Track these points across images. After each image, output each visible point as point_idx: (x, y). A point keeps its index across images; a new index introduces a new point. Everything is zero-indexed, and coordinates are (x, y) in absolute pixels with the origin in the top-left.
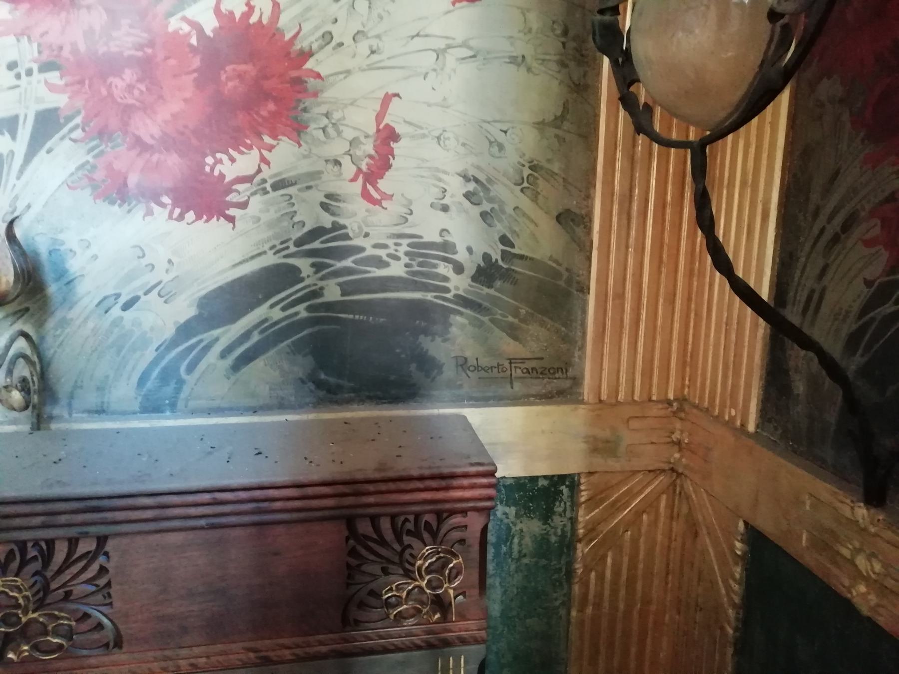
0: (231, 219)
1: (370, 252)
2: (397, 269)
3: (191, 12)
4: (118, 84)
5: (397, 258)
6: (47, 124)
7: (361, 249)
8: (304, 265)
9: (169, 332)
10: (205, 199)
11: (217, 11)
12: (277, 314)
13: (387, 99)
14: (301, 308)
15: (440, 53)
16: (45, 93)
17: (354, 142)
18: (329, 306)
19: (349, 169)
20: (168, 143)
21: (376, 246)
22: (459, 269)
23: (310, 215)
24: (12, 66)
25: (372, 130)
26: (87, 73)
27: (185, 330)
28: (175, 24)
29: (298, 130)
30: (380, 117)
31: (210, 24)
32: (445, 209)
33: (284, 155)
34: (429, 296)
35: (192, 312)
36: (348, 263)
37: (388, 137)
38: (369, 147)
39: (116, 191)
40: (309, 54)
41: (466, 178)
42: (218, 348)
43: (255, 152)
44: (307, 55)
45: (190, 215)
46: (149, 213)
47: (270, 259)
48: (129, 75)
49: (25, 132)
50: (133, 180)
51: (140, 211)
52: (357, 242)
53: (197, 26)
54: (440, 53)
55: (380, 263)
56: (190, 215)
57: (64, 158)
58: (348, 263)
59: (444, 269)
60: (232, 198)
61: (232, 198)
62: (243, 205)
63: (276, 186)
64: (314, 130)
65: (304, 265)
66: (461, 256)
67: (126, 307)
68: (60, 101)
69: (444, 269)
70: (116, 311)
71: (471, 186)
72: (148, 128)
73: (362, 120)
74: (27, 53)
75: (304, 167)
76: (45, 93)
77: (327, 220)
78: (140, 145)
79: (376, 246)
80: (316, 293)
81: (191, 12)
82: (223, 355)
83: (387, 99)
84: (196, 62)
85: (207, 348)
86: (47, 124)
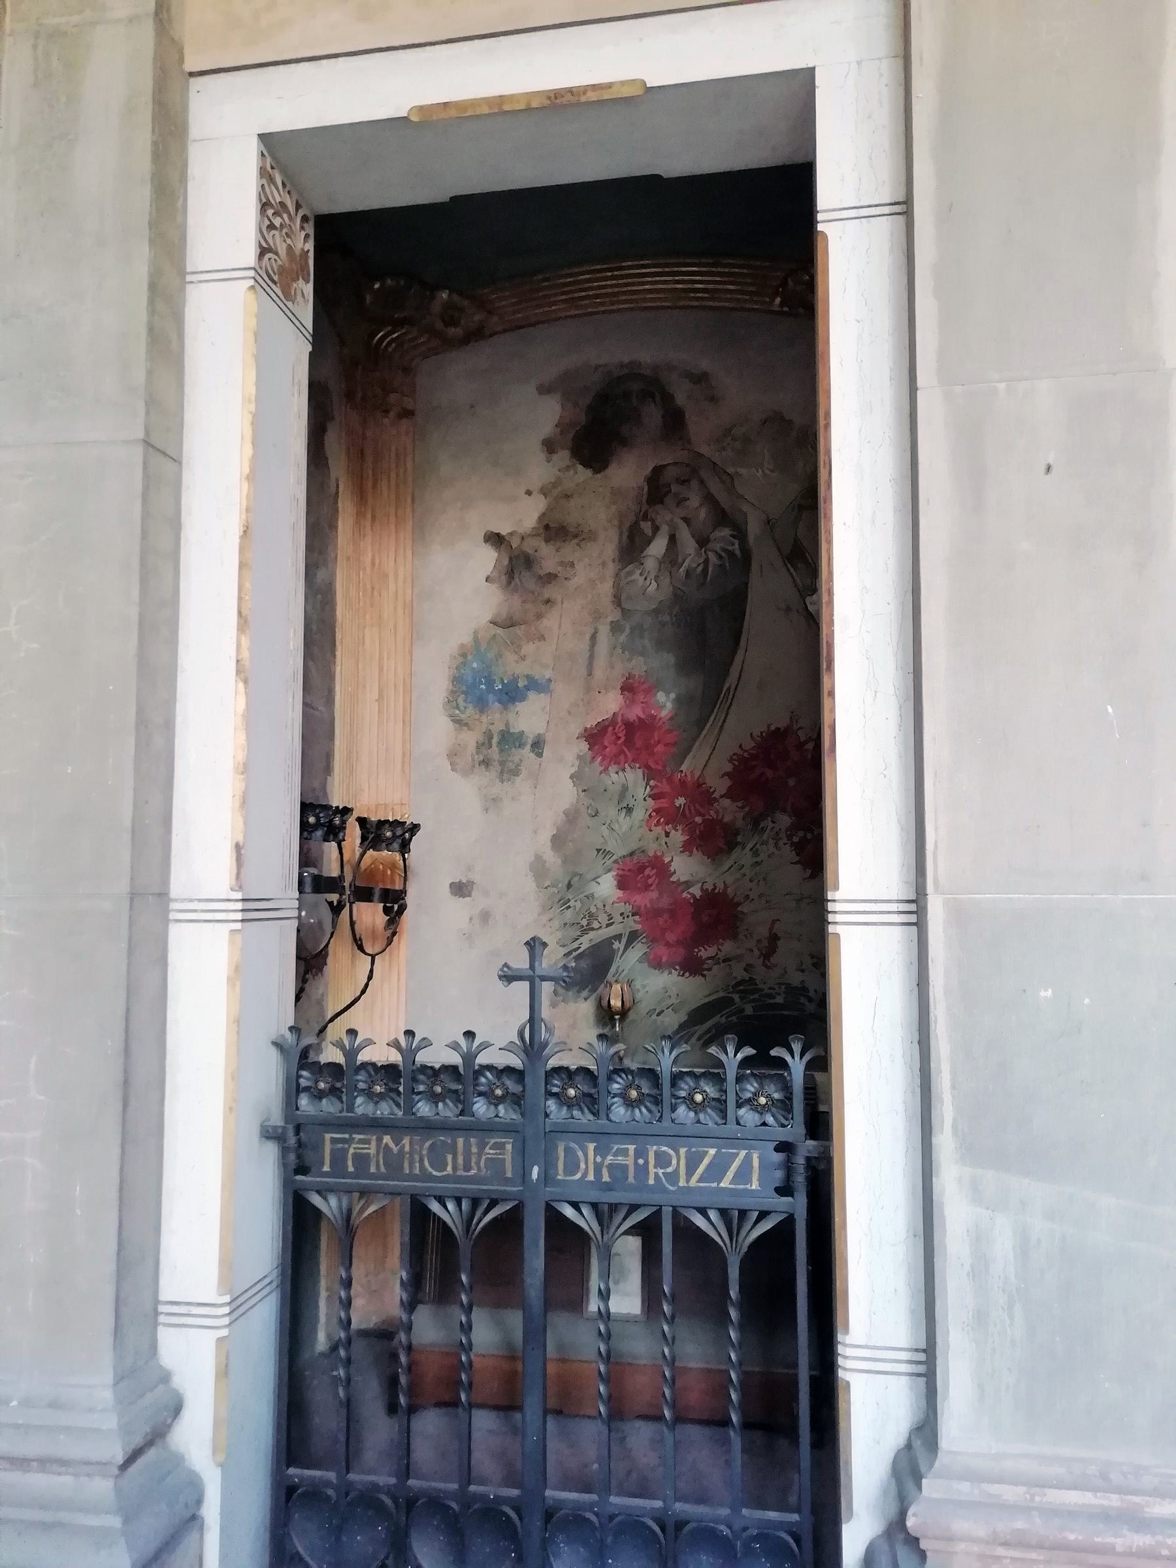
0: (704, 976)
1: (766, 991)
2: (779, 1000)
3: (690, 890)
4: (661, 921)
5: (779, 994)
6: (633, 937)
7: (762, 990)
8: (736, 997)
9: (676, 1027)
10: (692, 967)
11: (702, 889)
12: (723, 1020)
13: (774, 922)
14: (734, 1018)
15: (799, 901)
16: (633, 924)
17: (759, 941)
18: (748, 1017)
19: (756, 952)
20: (679, 942)
21: (770, 988)
22: (810, 1000)
23: (739, 973)
24: (622, 914)
25: (767, 935)
26: (648, 915)
27: (682, 1027)
28: (684, 895)
29: (734, 937)
30: (771, 929)
31: (698, 893)
32: (803, 971)
33: (728, 947)
34: (796, 1013)
35: (685, 1018)
36: (756, 996)
37: (774, 938)
38: (765, 943)
39: (657, 964)
40: (739, 904)
41: (812, 957)
42: (696, 1036)
43: (715, 947)
44: (739, 904)
45: (687, 974)
46: (670, 973)
47: (721, 994)
48: (666, 916)
49: (624, 940)
50: (664, 959)
51: (666, 972)
52: (760, 986)
53: (694, 896)
54: (799, 901)
55: (772, 997)
56: (687, 974)
57: (637, 951)
58: (756, 996)
59: (802, 1000)
60: (706, 966)
61: (706, 966)
62: (709, 970)
63: (724, 961)
64: (741, 936)
65: (736, 997)
66: (812, 994)
67: (658, 1015)
68: (639, 927)
69: (802, 1000)
70: (654, 1017)
71: (815, 960)
72: (671, 937)
73: (763, 931)
74: (629, 908)
75: (739, 952)
76: (633, 924)
77: (746, 976)
78: (668, 944)
79: (770, 988)
80: (743, 1010)
81: (690, 890)
82: (699, 1039)
83: (774, 922)
84: (692, 910)
85: (693, 1035)
86: (633, 937)
